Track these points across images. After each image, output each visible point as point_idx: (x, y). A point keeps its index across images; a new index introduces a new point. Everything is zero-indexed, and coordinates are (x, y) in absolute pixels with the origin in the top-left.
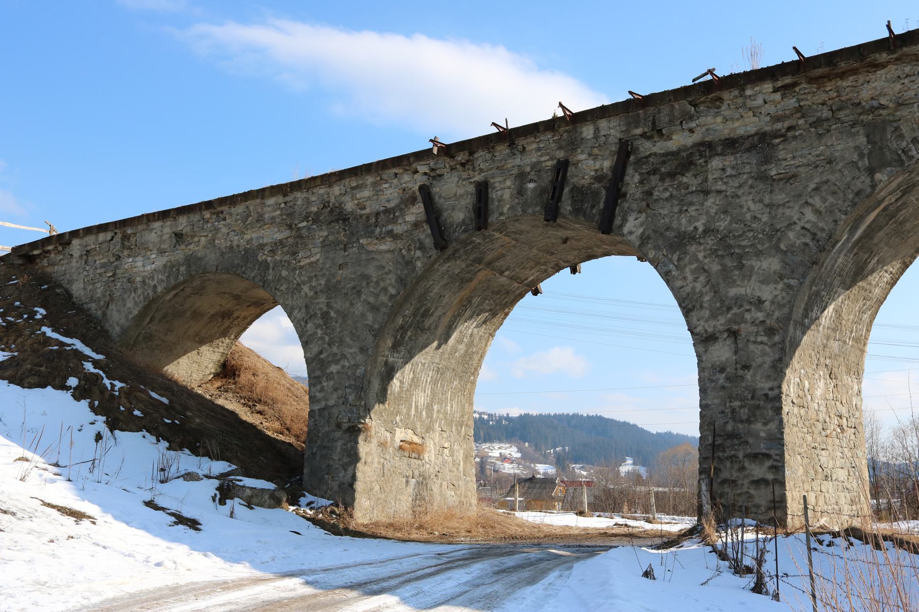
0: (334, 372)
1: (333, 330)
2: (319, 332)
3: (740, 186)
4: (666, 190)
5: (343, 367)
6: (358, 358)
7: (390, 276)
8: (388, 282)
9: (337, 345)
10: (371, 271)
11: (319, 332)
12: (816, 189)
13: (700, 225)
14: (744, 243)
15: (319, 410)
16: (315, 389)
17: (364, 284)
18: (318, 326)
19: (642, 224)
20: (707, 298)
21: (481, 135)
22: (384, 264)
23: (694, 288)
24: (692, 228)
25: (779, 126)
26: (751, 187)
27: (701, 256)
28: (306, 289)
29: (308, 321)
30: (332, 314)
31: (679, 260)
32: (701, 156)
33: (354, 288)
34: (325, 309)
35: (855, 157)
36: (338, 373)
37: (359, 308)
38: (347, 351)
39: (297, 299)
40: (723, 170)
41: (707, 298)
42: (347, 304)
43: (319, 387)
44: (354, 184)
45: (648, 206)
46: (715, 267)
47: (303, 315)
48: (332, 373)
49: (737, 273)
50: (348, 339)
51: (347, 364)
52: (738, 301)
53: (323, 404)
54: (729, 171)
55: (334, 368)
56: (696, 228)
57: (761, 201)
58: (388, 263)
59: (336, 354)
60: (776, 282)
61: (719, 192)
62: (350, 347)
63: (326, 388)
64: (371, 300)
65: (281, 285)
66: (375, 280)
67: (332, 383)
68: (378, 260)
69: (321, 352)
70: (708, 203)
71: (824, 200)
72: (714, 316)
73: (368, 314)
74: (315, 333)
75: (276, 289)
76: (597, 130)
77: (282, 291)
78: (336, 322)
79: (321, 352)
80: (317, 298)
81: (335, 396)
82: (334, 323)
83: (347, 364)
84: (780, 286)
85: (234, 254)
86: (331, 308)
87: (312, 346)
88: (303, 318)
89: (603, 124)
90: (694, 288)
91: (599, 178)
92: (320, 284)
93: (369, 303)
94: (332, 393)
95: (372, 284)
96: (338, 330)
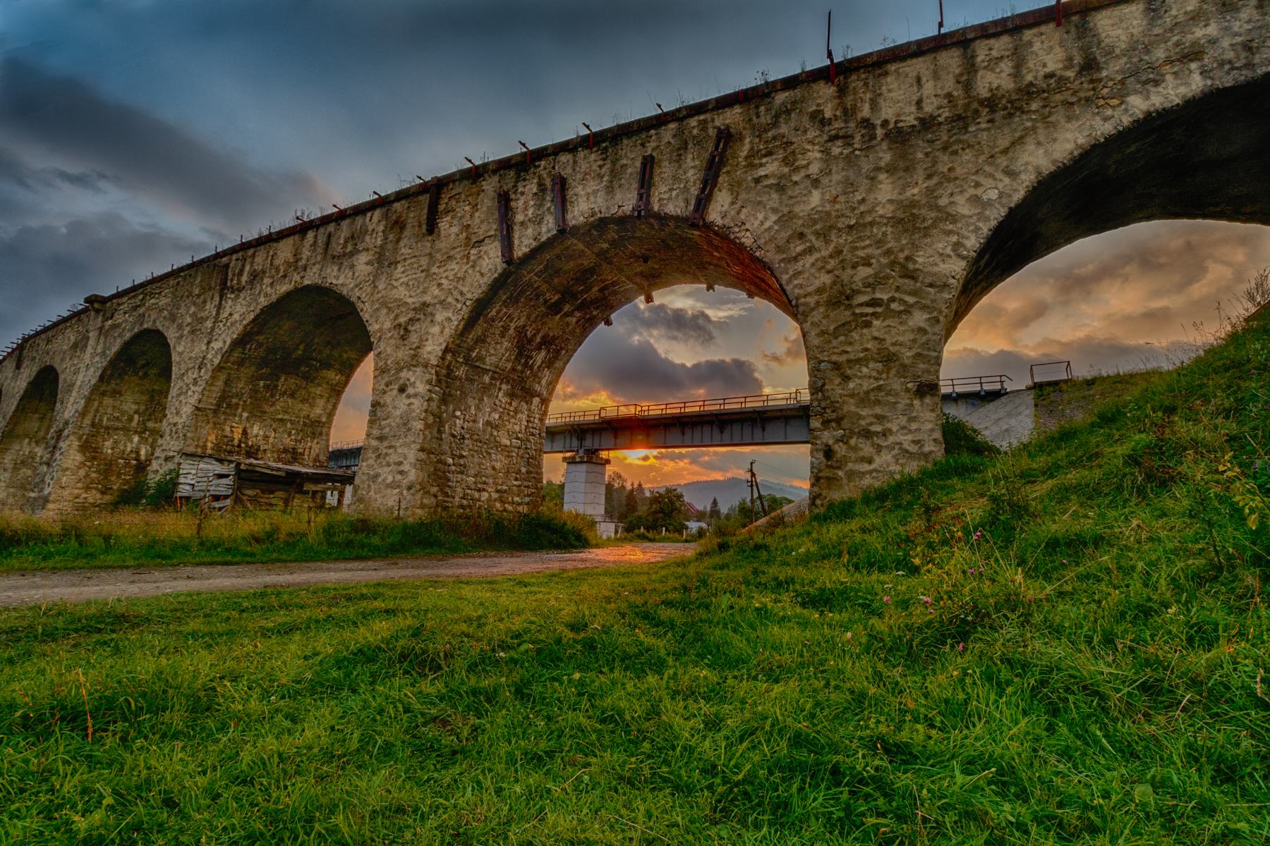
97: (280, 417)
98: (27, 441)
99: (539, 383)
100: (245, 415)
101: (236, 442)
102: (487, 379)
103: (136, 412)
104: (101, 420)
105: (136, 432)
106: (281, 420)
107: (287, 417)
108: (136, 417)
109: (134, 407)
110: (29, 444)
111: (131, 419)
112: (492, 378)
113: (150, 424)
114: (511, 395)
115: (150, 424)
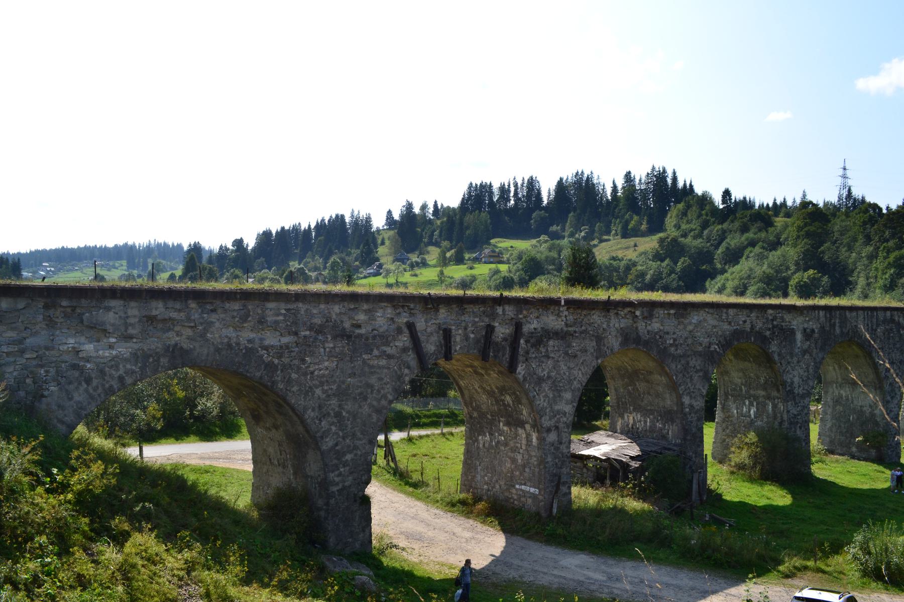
0: (349, 459)
1: (346, 426)
2: (333, 428)
3: (560, 357)
4: (533, 353)
5: (356, 455)
6: (367, 447)
7: (388, 386)
8: (386, 390)
9: (350, 438)
10: (373, 380)
11: (333, 428)
12: (582, 363)
13: (545, 373)
14: (561, 385)
15: (338, 491)
16: (333, 475)
17: (369, 390)
18: (333, 424)
19: (524, 369)
20: (548, 411)
22: (383, 377)
23: (543, 405)
24: (543, 375)
25: (570, 329)
26: (563, 358)
27: (547, 389)
28: (318, 392)
29: (322, 419)
30: (344, 414)
31: (539, 390)
32: (546, 337)
33: (361, 394)
34: (337, 409)
35: (593, 350)
36: (352, 459)
37: (366, 409)
38: (358, 443)
39: (309, 400)
40: (554, 347)
41: (548, 411)
42: (357, 406)
43: (337, 473)
44: (352, 307)
45: (527, 360)
46: (551, 396)
47: (316, 414)
48: (347, 460)
49: (558, 399)
50: (359, 434)
51: (359, 453)
52: (558, 412)
53: (340, 486)
54: (556, 348)
55: (349, 457)
56: (544, 375)
57: (566, 365)
58: (386, 376)
59: (349, 446)
60: (570, 404)
61: (553, 358)
62: (360, 439)
63: (343, 473)
64: (375, 403)
65: (293, 387)
66: (377, 388)
67: (347, 468)
68: (378, 373)
69: (336, 445)
70: (549, 362)
71: (584, 368)
72: (550, 419)
73: (374, 414)
74: (329, 430)
75: (287, 390)
76: (504, 310)
77: (294, 392)
78: (348, 420)
79: (336, 445)
80: (329, 400)
81: (350, 478)
82: (346, 421)
83: (359, 453)
84: (571, 406)
85: (233, 351)
86: (343, 409)
87: (327, 440)
88: (317, 417)
89: (507, 307)
90: (543, 405)
91: (505, 339)
92: (332, 389)
93: (373, 406)
94: (348, 476)
95: (375, 391)
96: (350, 426)
97: (649, 408)
98: (835, 385)
99: (522, 414)
100: (632, 408)
101: (630, 426)
102: (489, 417)
103: (742, 384)
104: (728, 391)
105: (746, 398)
106: (650, 410)
107: (653, 408)
108: (743, 387)
109: (739, 381)
110: (836, 387)
111: (741, 389)
112: (492, 416)
113: (752, 392)
114: (508, 424)
115: (752, 392)
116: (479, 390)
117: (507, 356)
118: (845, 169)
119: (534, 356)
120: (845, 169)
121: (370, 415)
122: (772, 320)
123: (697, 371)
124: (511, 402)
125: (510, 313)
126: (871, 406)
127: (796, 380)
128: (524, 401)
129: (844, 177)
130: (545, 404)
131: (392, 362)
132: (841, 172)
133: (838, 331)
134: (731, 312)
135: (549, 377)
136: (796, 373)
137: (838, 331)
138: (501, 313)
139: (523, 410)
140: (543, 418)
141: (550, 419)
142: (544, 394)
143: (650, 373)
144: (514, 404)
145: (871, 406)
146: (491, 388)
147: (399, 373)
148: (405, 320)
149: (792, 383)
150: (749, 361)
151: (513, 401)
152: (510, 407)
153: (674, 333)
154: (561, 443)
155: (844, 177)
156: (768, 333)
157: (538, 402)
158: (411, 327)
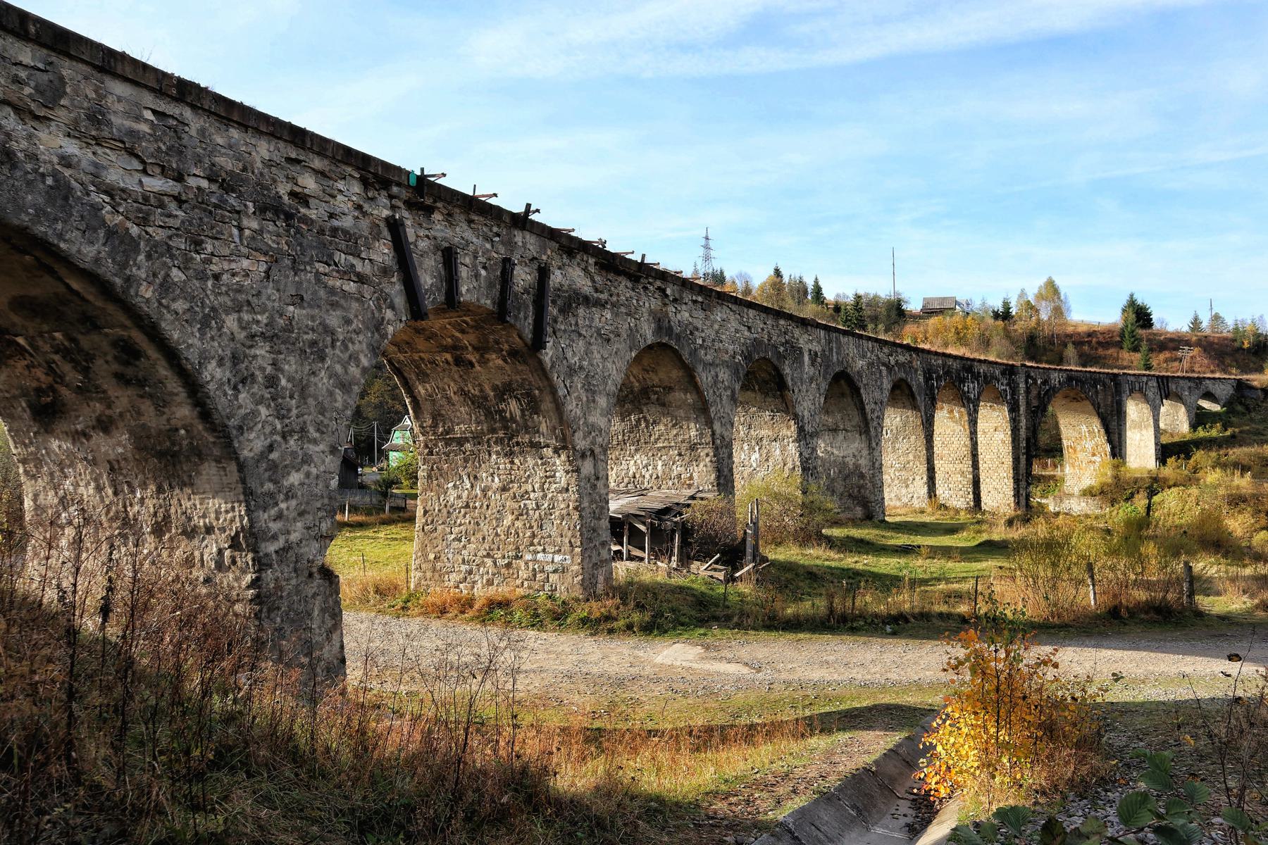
0: (296, 483)
1: (289, 410)
2: (264, 411)
5: (308, 475)
6: (327, 460)
7: (361, 337)
8: (357, 347)
9: (296, 437)
10: (333, 320)
11: (264, 411)
14: (595, 382)
15: (276, 552)
16: (266, 516)
17: (329, 339)
18: (261, 400)
21: (317, 132)
22: (352, 316)
28: (231, 322)
29: (240, 386)
30: (283, 382)
31: (571, 387)
33: (313, 343)
34: (269, 369)
36: (302, 484)
37: (322, 382)
38: (312, 448)
39: (212, 338)
43: (273, 512)
44: (293, 156)
47: (228, 374)
48: (292, 485)
50: (311, 430)
51: (314, 471)
53: (281, 543)
55: (295, 478)
58: (356, 316)
59: (294, 454)
62: (315, 442)
63: (285, 512)
64: (338, 368)
65: (174, 300)
66: (341, 338)
67: (293, 503)
68: (342, 307)
69: (271, 448)
73: (337, 390)
74: (255, 413)
75: (160, 304)
77: (177, 313)
78: (291, 397)
79: (271, 448)
80: (251, 347)
81: (299, 524)
82: (288, 399)
83: (314, 471)
85: (18, 173)
86: (282, 371)
87: (252, 436)
88: (229, 380)
91: (526, 291)
92: (258, 322)
93: (336, 375)
94: (295, 520)
95: (338, 344)
96: (294, 412)
116: (455, 398)
117: (530, 320)
118: (707, 238)
119: (563, 328)
120: (707, 238)
121: (331, 394)
122: (785, 333)
123: (725, 389)
124: (518, 413)
125: (531, 248)
126: (854, 456)
127: (806, 413)
128: (547, 405)
129: (707, 247)
130: (578, 412)
131: (367, 291)
132: (703, 242)
133: (835, 358)
134: (752, 313)
135: (581, 368)
136: (805, 404)
137: (835, 358)
138: (520, 244)
139: (540, 423)
140: (576, 434)
141: (584, 438)
142: (576, 395)
143: (670, 389)
144: (523, 415)
145: (854, 456)
146: (481, 391)
147: (377, 315)
148: (386, 213)
149: (803, 417)
150: (754, 390)
151: (522, 411)
152: (515, 421)
153: (703, 331)
154: (598, 478)
155: (707, 247)
156: (782, 349)
157: (570, 408)
158: (395, 227)
